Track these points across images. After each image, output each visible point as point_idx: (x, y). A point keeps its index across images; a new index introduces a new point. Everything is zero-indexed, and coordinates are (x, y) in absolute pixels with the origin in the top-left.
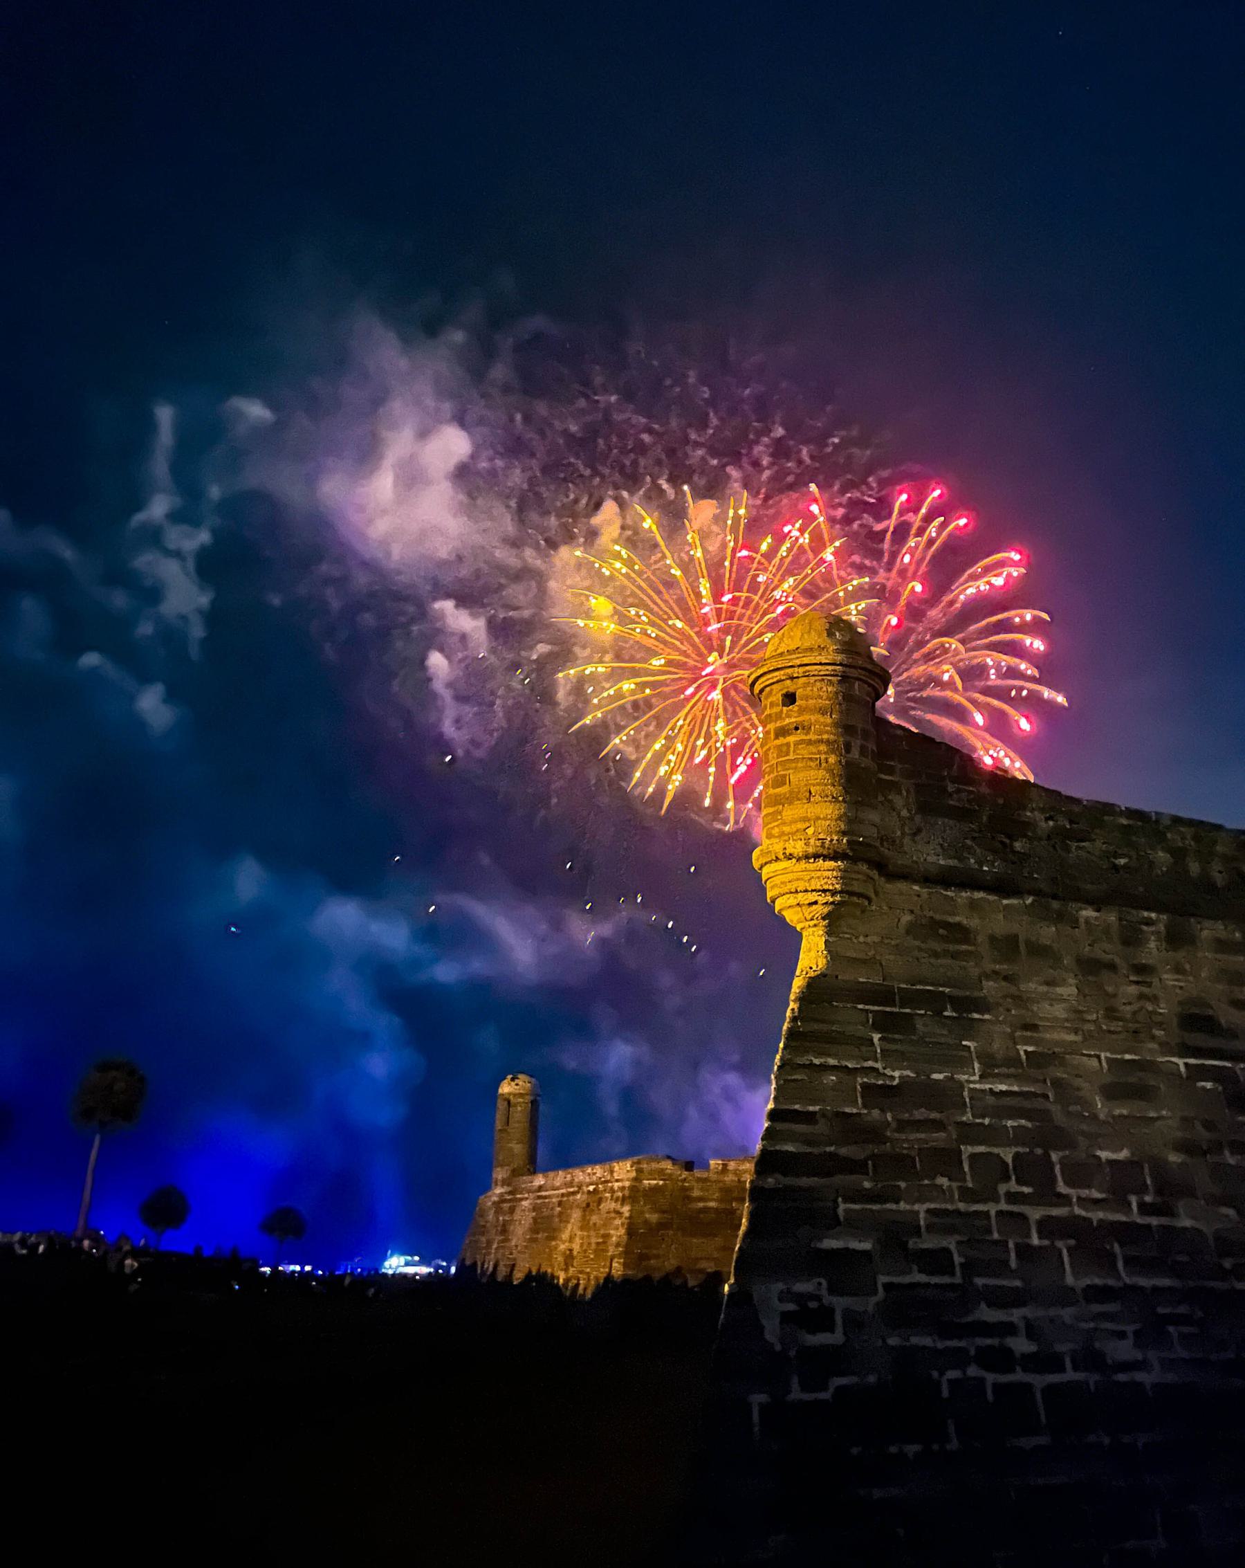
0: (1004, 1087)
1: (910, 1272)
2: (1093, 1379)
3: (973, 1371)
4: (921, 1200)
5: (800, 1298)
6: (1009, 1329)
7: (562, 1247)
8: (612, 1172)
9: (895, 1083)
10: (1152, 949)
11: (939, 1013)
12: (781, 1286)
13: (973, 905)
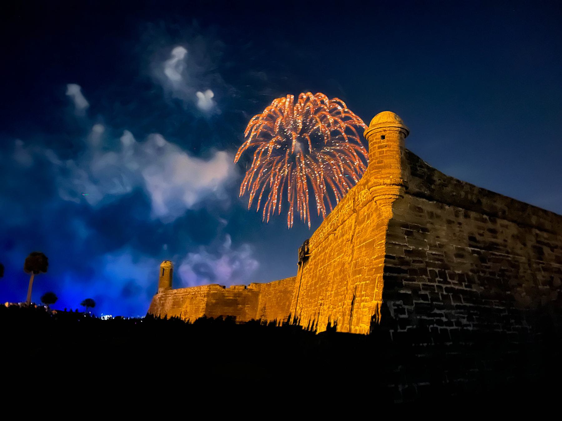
0: (434, 253)
1: (419, 300)
2: (460, 328)
3: (435, 326)
4: (422, 281)
5: (398, 306)
7: (183, 310)
8: (200, 289)
10: (461, 219)
11: (418, 232)
12: (392, 302)
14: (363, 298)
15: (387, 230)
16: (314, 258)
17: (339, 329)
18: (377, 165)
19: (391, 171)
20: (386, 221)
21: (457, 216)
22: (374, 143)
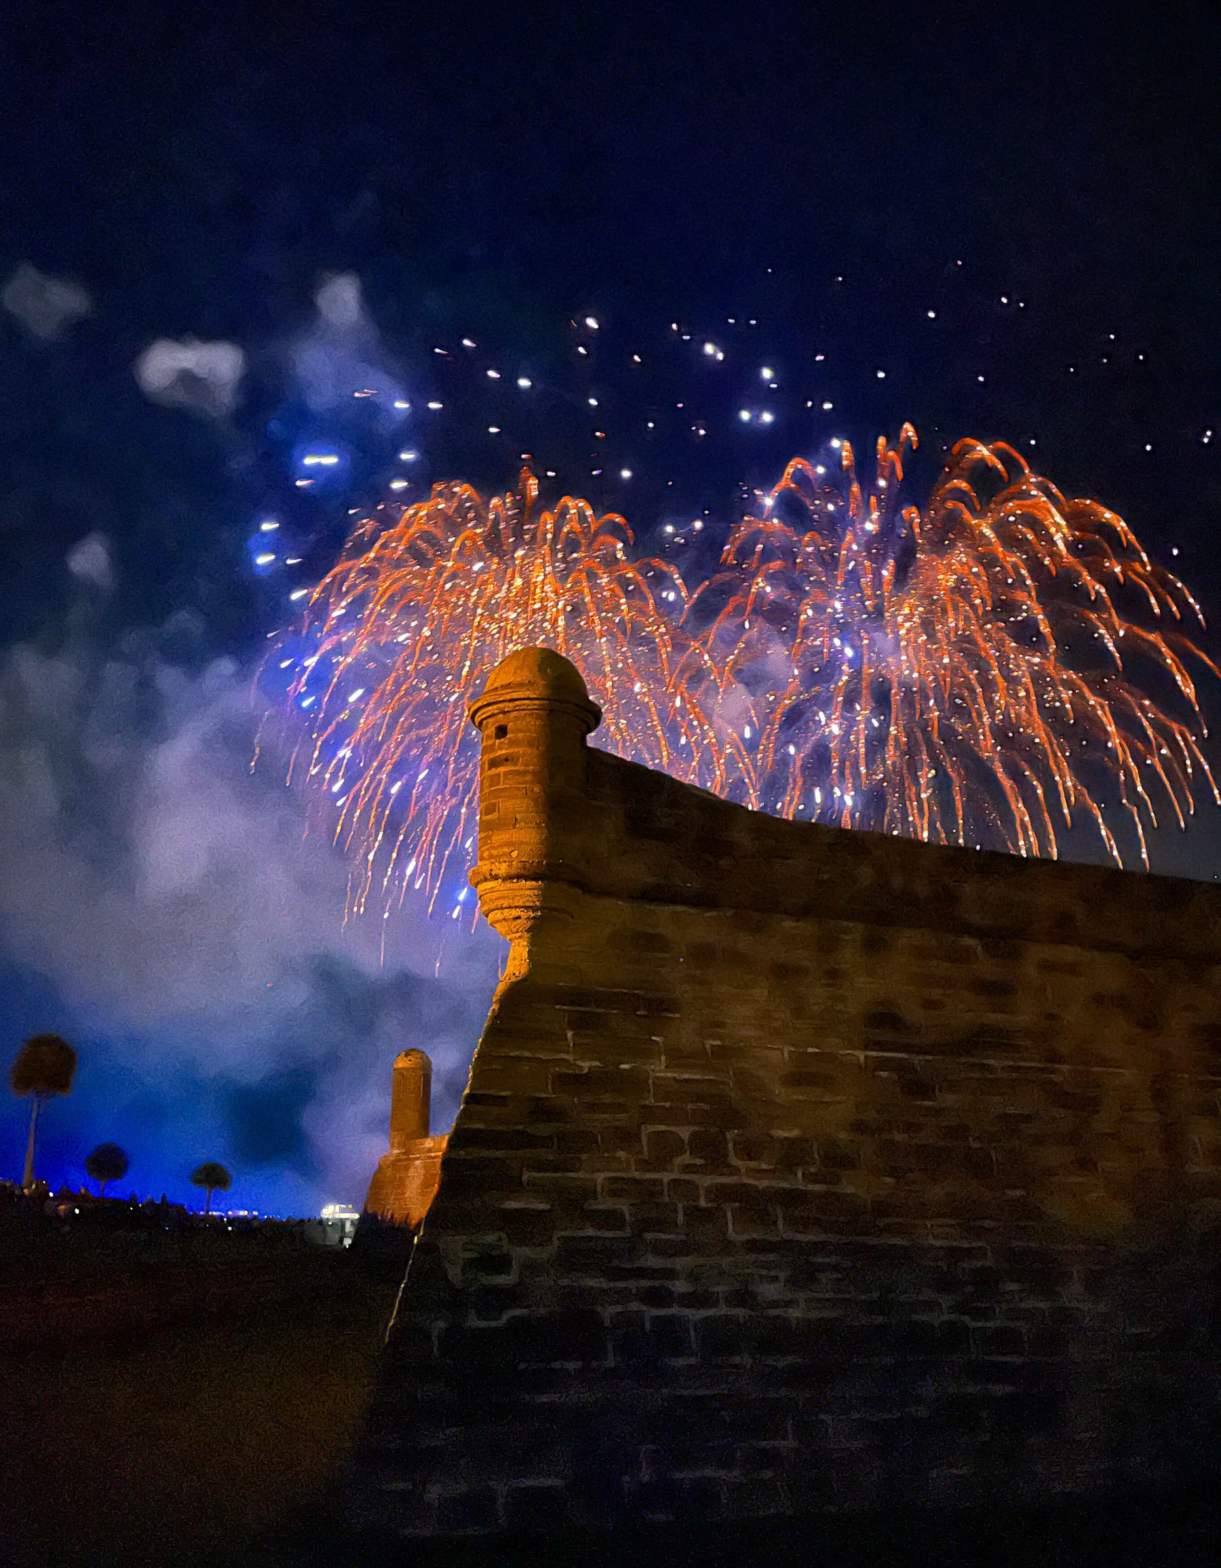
0: (686, 1076)
2: (741, 1313)
6: (670, 1274)
9: (586, 1071)
10: (849, 956)
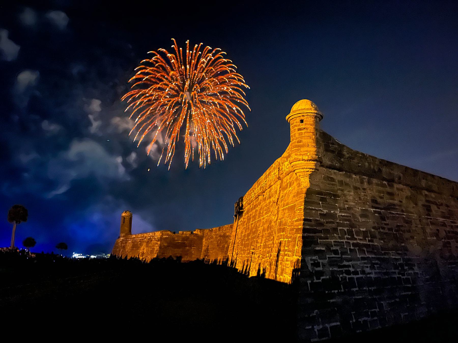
0: (343, 215)
2: (364, 276)
5: (314, 260)
10: (366, 185)
11: (331, 198)
12: (310, 258)
13: (335, 173)
14: (286, 253)
15: (305, 198)
16: (248, 212)
17: (267, 276)
18: (297, 144)
19: (309, 149)
20: (305, 190)
21: (362, 182)
22: (294, 126)
